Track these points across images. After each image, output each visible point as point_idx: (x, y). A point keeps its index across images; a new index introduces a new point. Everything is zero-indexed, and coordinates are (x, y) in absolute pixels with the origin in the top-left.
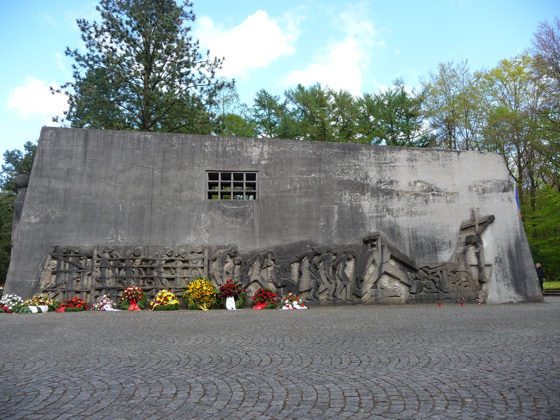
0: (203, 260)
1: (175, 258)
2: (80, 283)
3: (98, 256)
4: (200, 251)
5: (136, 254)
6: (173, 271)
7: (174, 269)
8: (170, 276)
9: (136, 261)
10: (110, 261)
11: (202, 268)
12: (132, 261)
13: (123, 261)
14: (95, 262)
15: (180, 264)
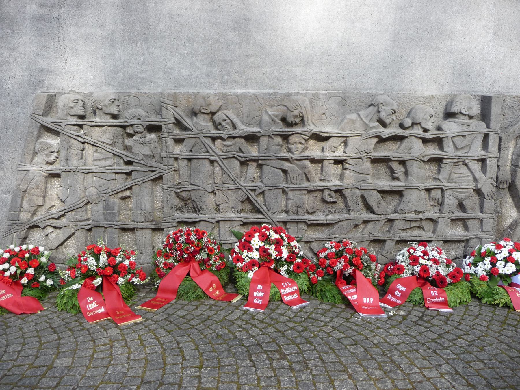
0: (486, 136)
1: (406, 133)
2: (131, 203)
3: (178, 123)
5: (290, 119)
6: (399, 170)
7: (402, 163)
8: (385, 183)
9: (292, 139)
10: (214, 139)
11: (483, 161)
12: (279, 140)
13: (252, 138)
14: (170, 142)
15: (418, 149)
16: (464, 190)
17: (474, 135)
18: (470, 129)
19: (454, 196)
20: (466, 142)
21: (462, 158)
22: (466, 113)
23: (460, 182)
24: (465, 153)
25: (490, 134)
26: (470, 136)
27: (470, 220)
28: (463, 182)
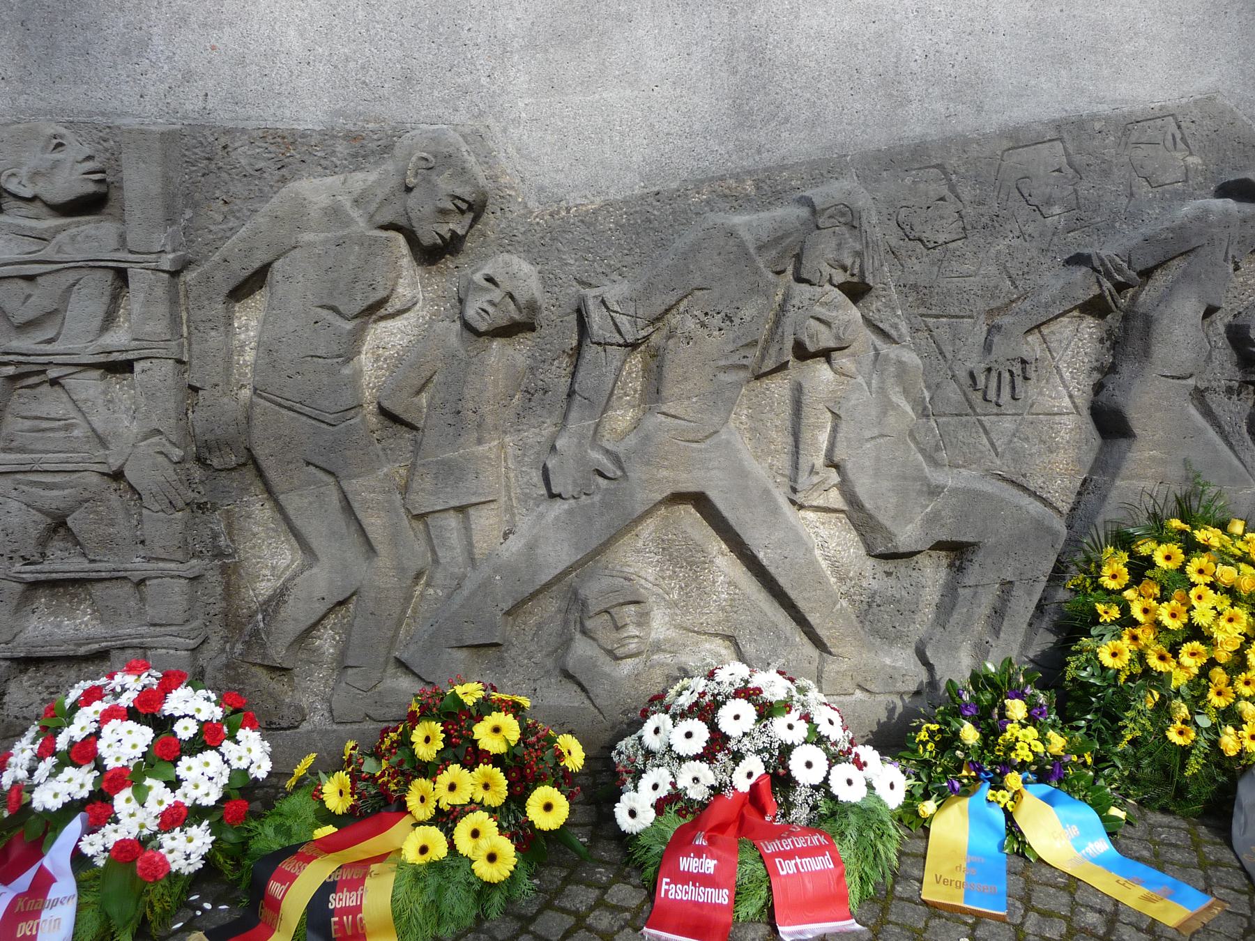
4: (70, 182)
16: (58, 479)
17: (71, 276)
18: (49, 252)
19: (22, 498)
20: (40, 298)
21: (31, 359)
22: (27, 192)
23: (39, 446)
24: (50, 341)
25: (130, 272)
26: (50, 278)
27: (99, 586)
28: (50, 447)
